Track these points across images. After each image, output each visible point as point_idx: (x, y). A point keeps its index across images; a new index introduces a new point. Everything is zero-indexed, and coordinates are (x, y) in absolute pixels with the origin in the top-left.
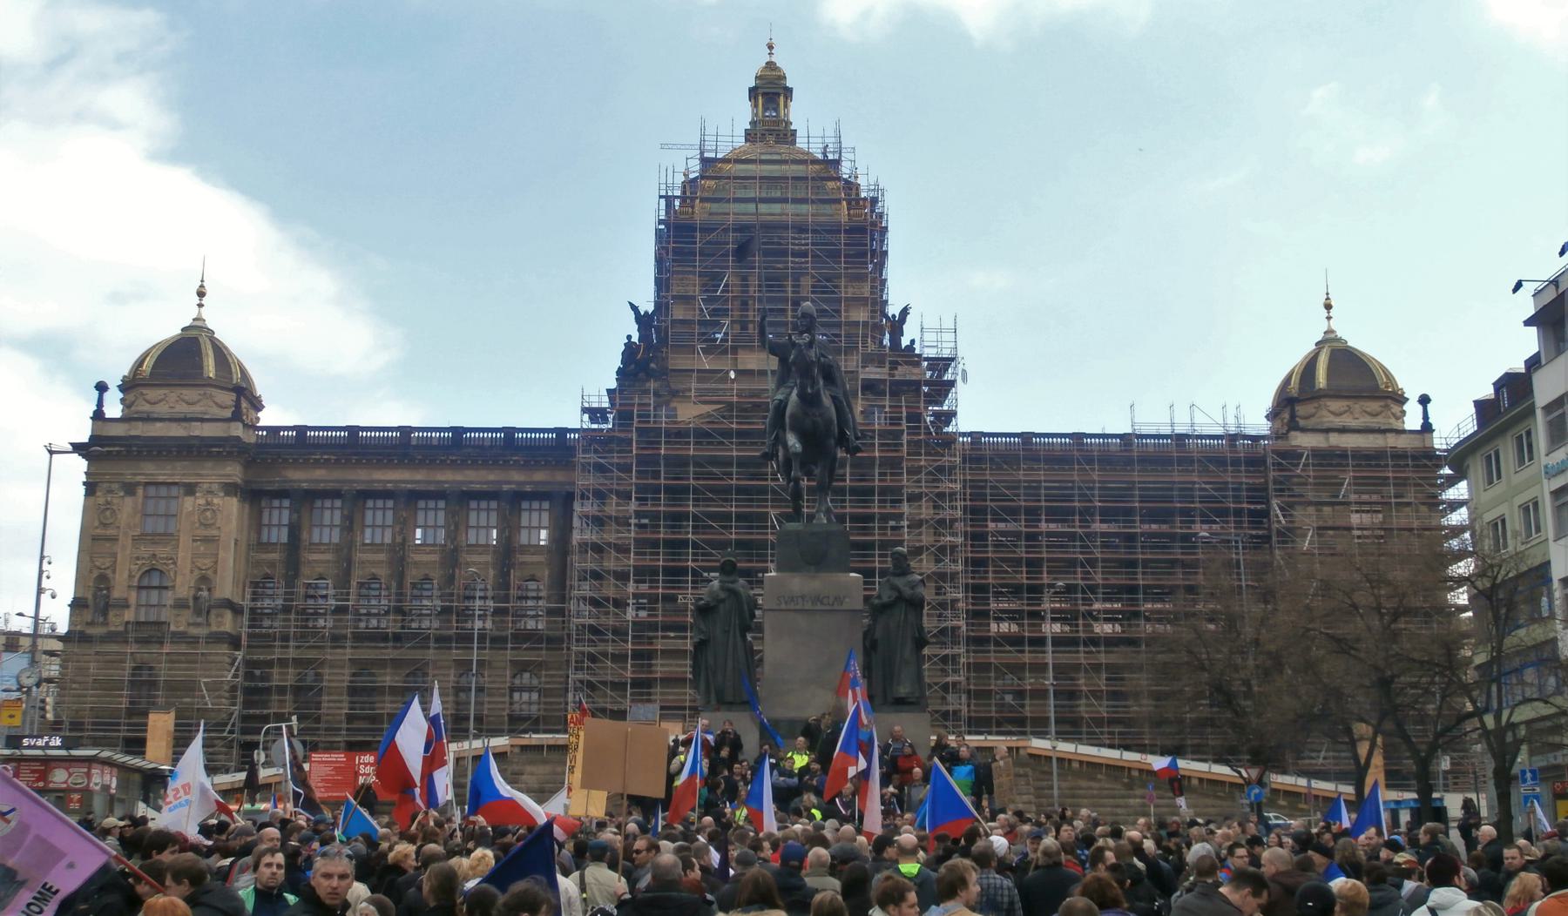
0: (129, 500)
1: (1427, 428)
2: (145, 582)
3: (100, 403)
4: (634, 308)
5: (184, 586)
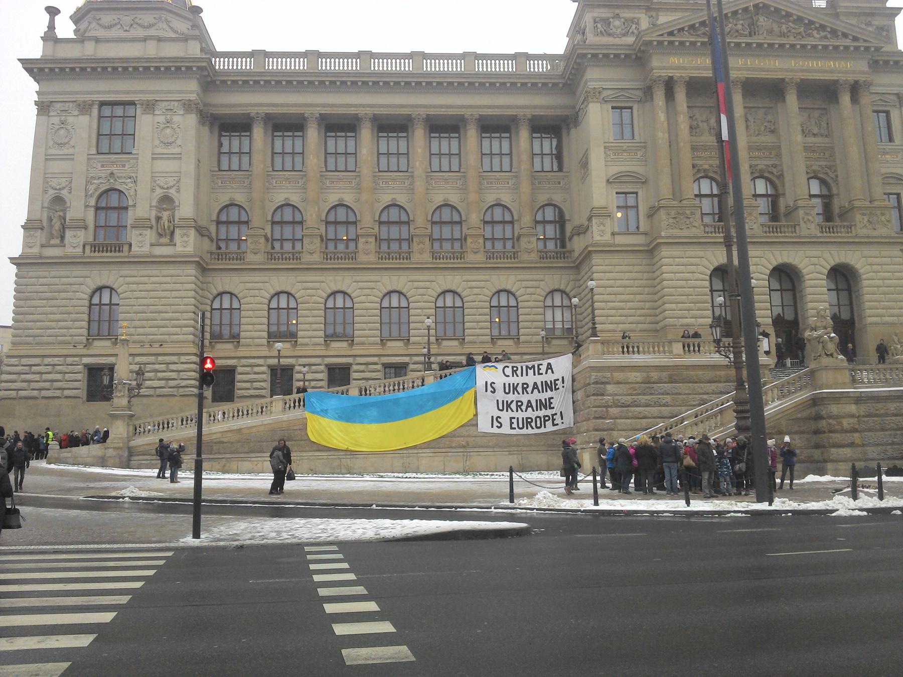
0: (85, 119)
2: (104, 205)
3: (51, 26)
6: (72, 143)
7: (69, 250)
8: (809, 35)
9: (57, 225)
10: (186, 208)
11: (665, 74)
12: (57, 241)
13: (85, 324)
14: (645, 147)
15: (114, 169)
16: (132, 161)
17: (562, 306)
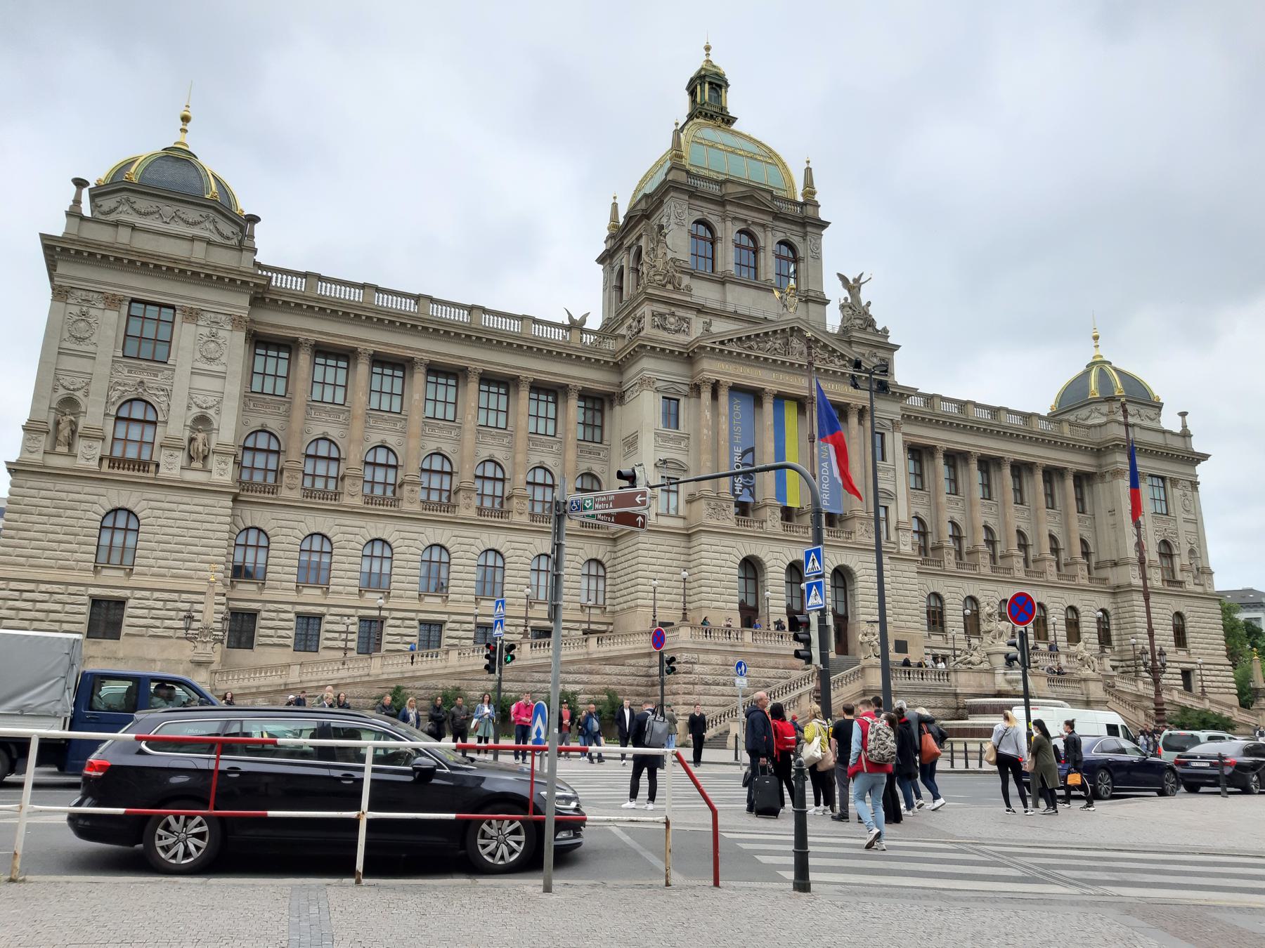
0: (112, 316)
1: (1186, 434)
3: (77, 201)
5: (177, 425)
6: (94, 339)
7: (81, 463)
8: (831, 362)
9: (65, 432)
10: (226, 431)
11: (714, 377)
12: (65, 449)
13: (94, 549)
14: (688, 438)
15: (145, 377)
16: (166, 372)
17: (597, 576)
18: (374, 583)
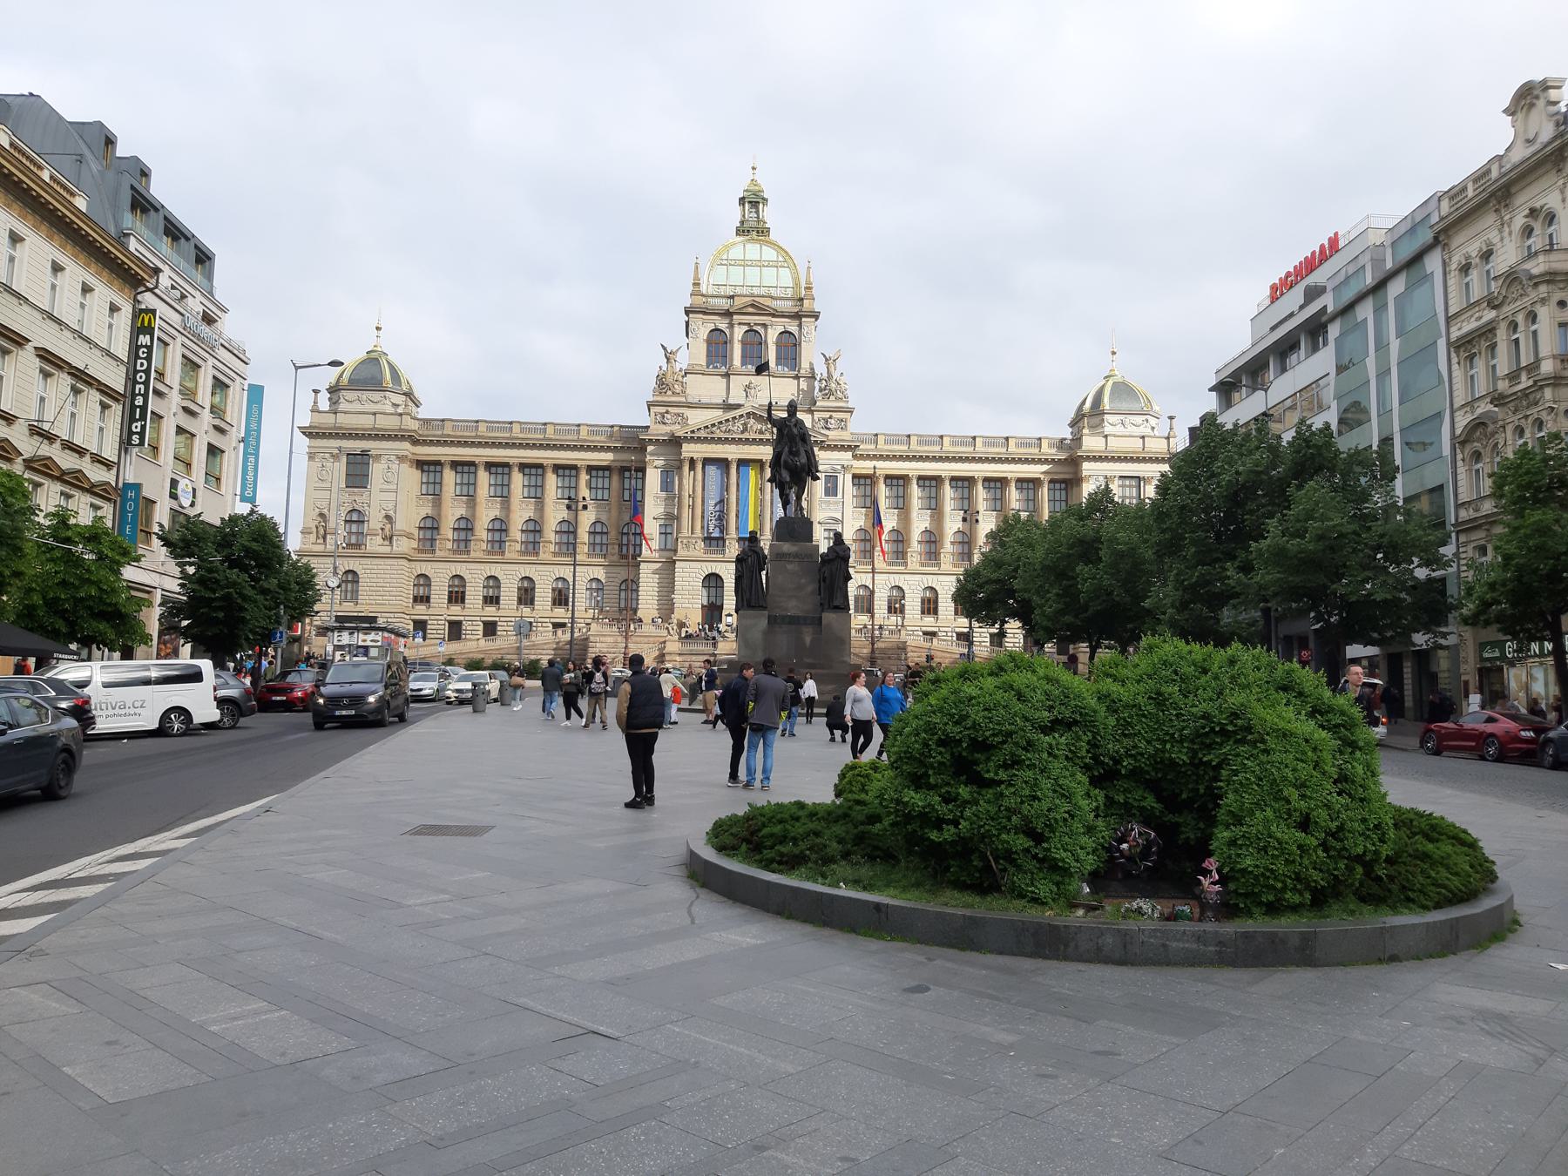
4: (664, 348)
9: (322, 532)
18: (492, 600)
